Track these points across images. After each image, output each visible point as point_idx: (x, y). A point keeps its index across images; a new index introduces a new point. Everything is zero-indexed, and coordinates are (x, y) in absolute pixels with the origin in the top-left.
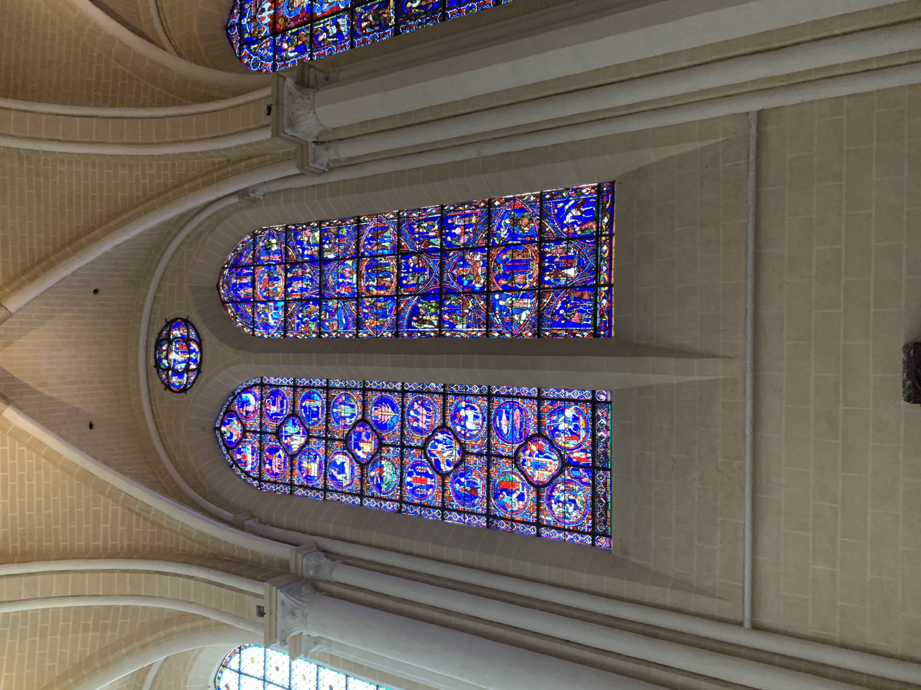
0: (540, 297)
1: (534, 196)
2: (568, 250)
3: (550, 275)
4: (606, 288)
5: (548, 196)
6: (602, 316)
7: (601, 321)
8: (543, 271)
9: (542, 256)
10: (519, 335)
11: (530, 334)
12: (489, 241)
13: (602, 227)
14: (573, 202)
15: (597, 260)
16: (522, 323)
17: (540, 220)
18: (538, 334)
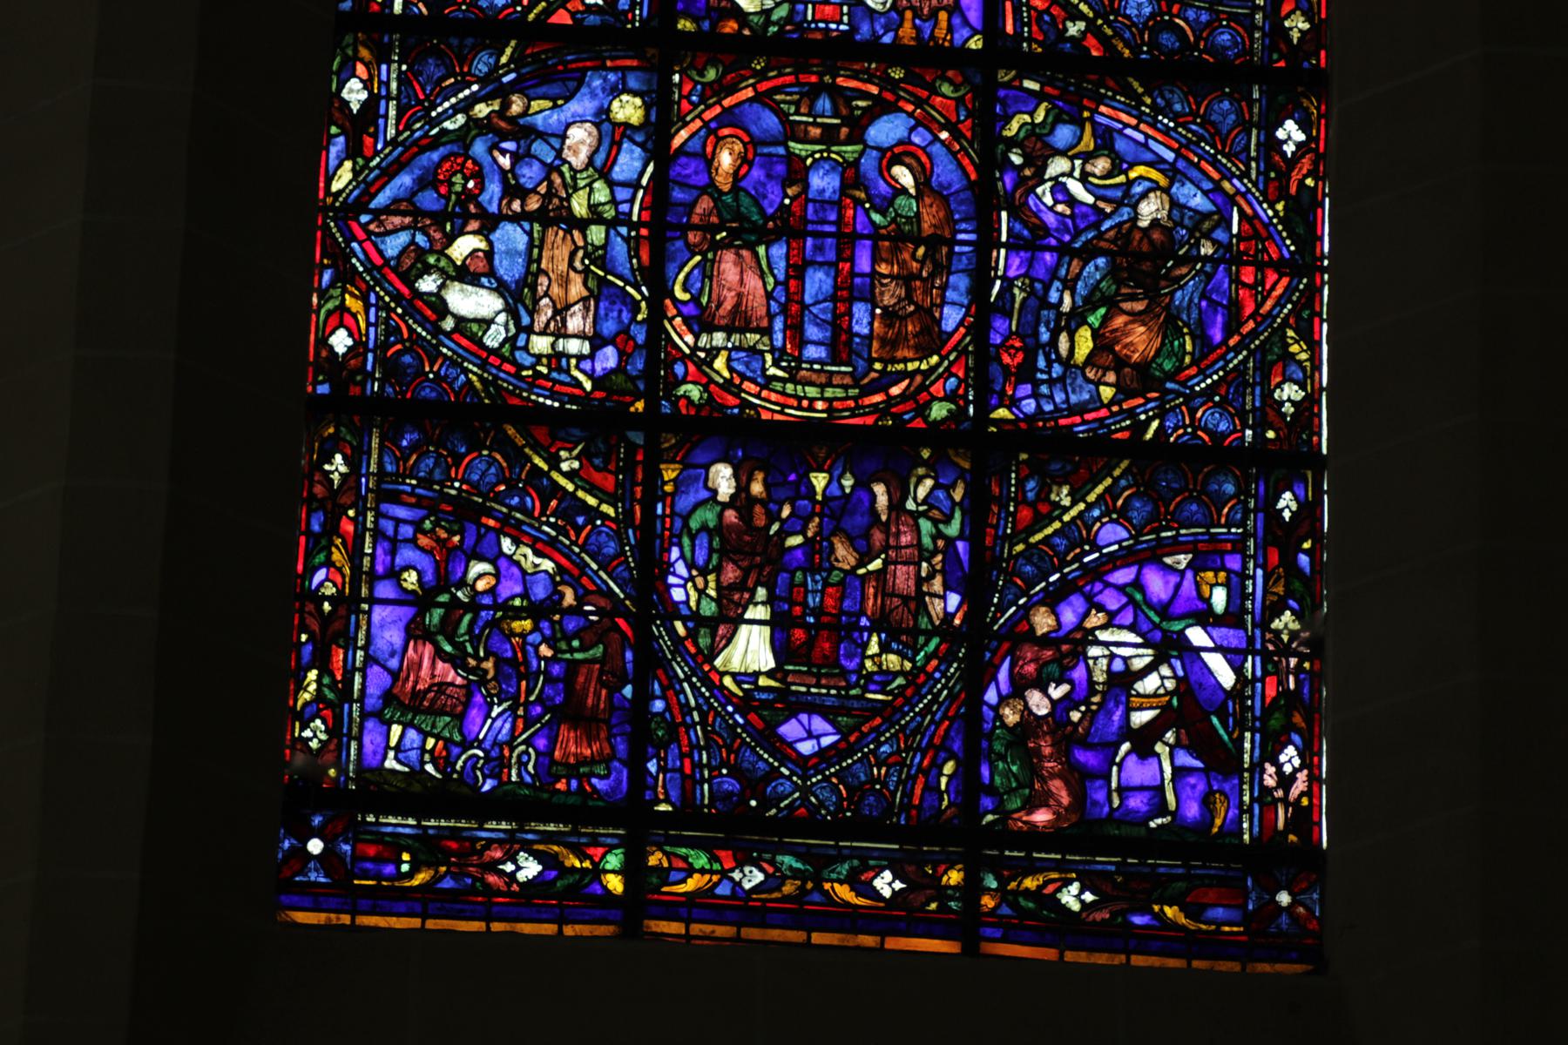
0: (597, 421)
1: (1306, 408)
2: (899, 635)
3: (742, 497)
4: (615, 884)
5: (1287, 502)
6: (427, 849)
7: (395, 844)
8: (775, 449)
9: (885, 448)
10: (340, 259)
11: (341, 341)
12: (1029, 66)
13: (1033, 868)
14: (1226, 678)
15: (813, 825)
16: (428, 284)
17: (1135, 446)
18: (351, 405)
